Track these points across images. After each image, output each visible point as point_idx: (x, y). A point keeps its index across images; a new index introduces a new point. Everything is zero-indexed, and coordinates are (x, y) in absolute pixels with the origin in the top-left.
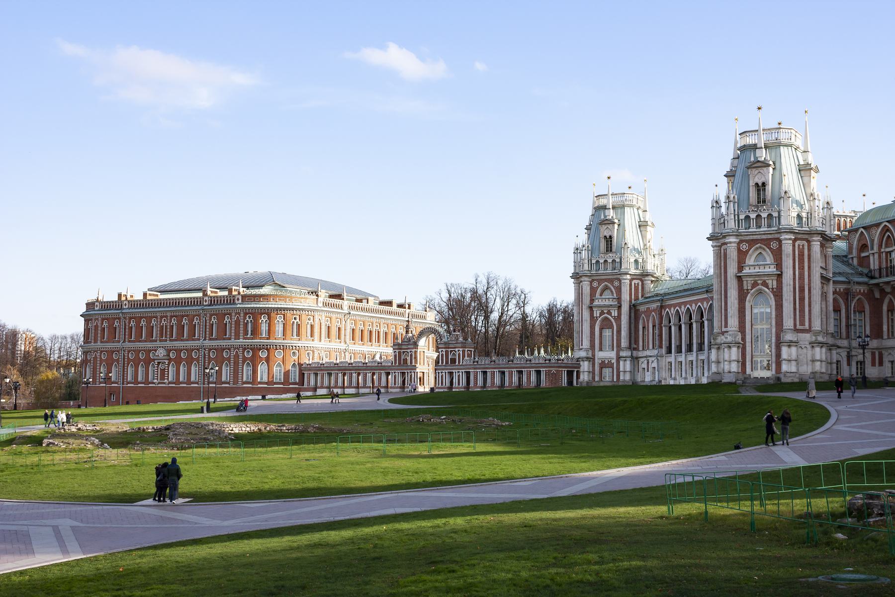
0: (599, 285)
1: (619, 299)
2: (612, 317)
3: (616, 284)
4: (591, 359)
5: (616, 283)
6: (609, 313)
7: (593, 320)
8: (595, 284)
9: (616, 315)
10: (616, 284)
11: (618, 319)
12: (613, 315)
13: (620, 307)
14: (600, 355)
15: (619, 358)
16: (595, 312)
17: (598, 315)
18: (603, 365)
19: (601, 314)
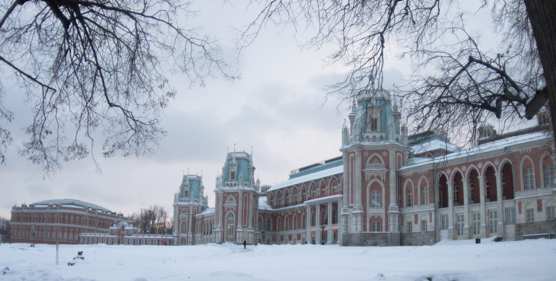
3: (385, 154)
8: (366, 154)
9: (385, 178)
10: (385, 154)
12: (382, 179)
14: (371, 212)
15: (386, 215)
17: (369, 179)
18: (372, 219)
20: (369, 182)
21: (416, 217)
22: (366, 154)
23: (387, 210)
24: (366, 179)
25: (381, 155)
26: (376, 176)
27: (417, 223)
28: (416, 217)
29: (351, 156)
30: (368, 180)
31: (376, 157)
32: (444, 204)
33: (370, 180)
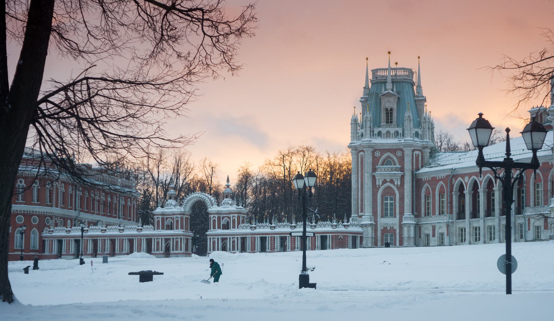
0: (382, 154)
1: (402, 169)
2: (395, 185)
4: (375, 227)
5: (399, 154)
6: (392, 181)
7: (375, 188)
8: (377, 154)
9: (399, 183)
11: (401, 187)
12: (396, 183)
13: (403, 177)
14: (384, 222)
15: (401, 227)
16: (377, 181)
17: (381, 183)
18: (385, 230)
19: (385, 182)
20: (380, 187)
21: (434, 230)
22: (377, 154)
23: (401, 220)
24: (377, 184)
25: (380, 157)
26: (388, 180)
27: (435, 237)
28: (434, 230)
29: (361, 155)
30: (379, 185)
31: (389, 157)
32: (461, 215)
33: (382, 186)
